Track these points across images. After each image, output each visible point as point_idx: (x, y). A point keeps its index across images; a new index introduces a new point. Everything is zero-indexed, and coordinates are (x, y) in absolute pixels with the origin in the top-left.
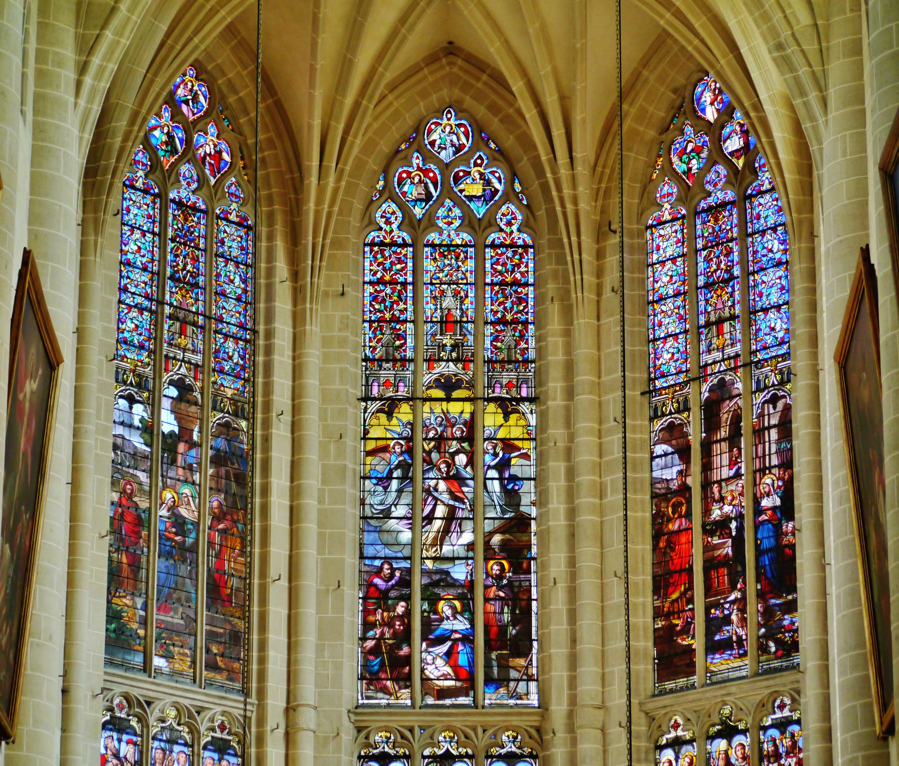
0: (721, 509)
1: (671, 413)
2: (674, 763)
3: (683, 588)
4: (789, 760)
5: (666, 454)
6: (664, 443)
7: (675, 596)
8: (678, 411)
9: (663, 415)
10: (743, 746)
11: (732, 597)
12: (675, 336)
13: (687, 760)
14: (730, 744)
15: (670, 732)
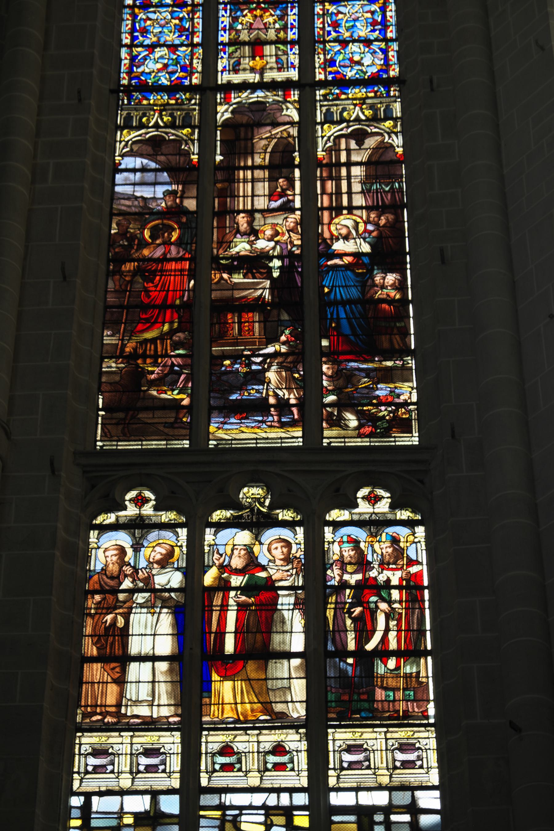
0: (251, 243)
1: (156, 126)
2: (130, 552)
3: (166, 327)
4: (387, 574)
5: (144, 170)
6: (141, 156)
7: (149, 335)
8: (172, 125)
9: (141, 126)
10: (288, 545)
11: (270, 350)
12: (173, 48)
13: (161, 551)
14: (257, 538)
15: (125, 508)
